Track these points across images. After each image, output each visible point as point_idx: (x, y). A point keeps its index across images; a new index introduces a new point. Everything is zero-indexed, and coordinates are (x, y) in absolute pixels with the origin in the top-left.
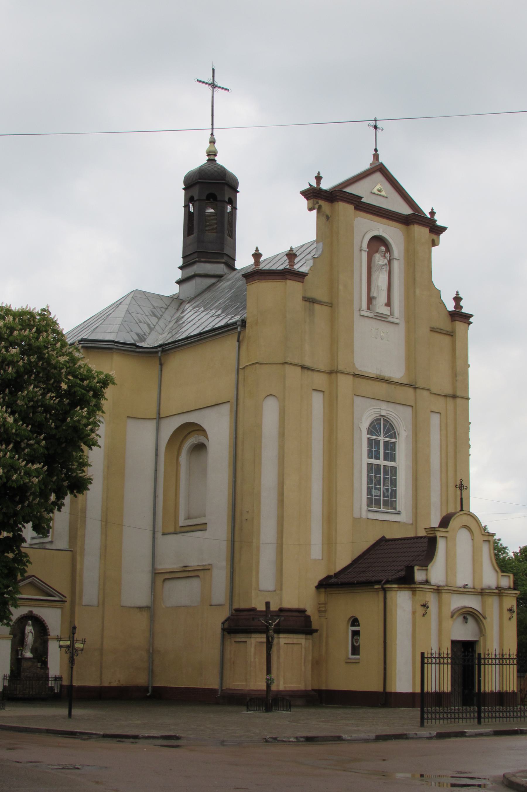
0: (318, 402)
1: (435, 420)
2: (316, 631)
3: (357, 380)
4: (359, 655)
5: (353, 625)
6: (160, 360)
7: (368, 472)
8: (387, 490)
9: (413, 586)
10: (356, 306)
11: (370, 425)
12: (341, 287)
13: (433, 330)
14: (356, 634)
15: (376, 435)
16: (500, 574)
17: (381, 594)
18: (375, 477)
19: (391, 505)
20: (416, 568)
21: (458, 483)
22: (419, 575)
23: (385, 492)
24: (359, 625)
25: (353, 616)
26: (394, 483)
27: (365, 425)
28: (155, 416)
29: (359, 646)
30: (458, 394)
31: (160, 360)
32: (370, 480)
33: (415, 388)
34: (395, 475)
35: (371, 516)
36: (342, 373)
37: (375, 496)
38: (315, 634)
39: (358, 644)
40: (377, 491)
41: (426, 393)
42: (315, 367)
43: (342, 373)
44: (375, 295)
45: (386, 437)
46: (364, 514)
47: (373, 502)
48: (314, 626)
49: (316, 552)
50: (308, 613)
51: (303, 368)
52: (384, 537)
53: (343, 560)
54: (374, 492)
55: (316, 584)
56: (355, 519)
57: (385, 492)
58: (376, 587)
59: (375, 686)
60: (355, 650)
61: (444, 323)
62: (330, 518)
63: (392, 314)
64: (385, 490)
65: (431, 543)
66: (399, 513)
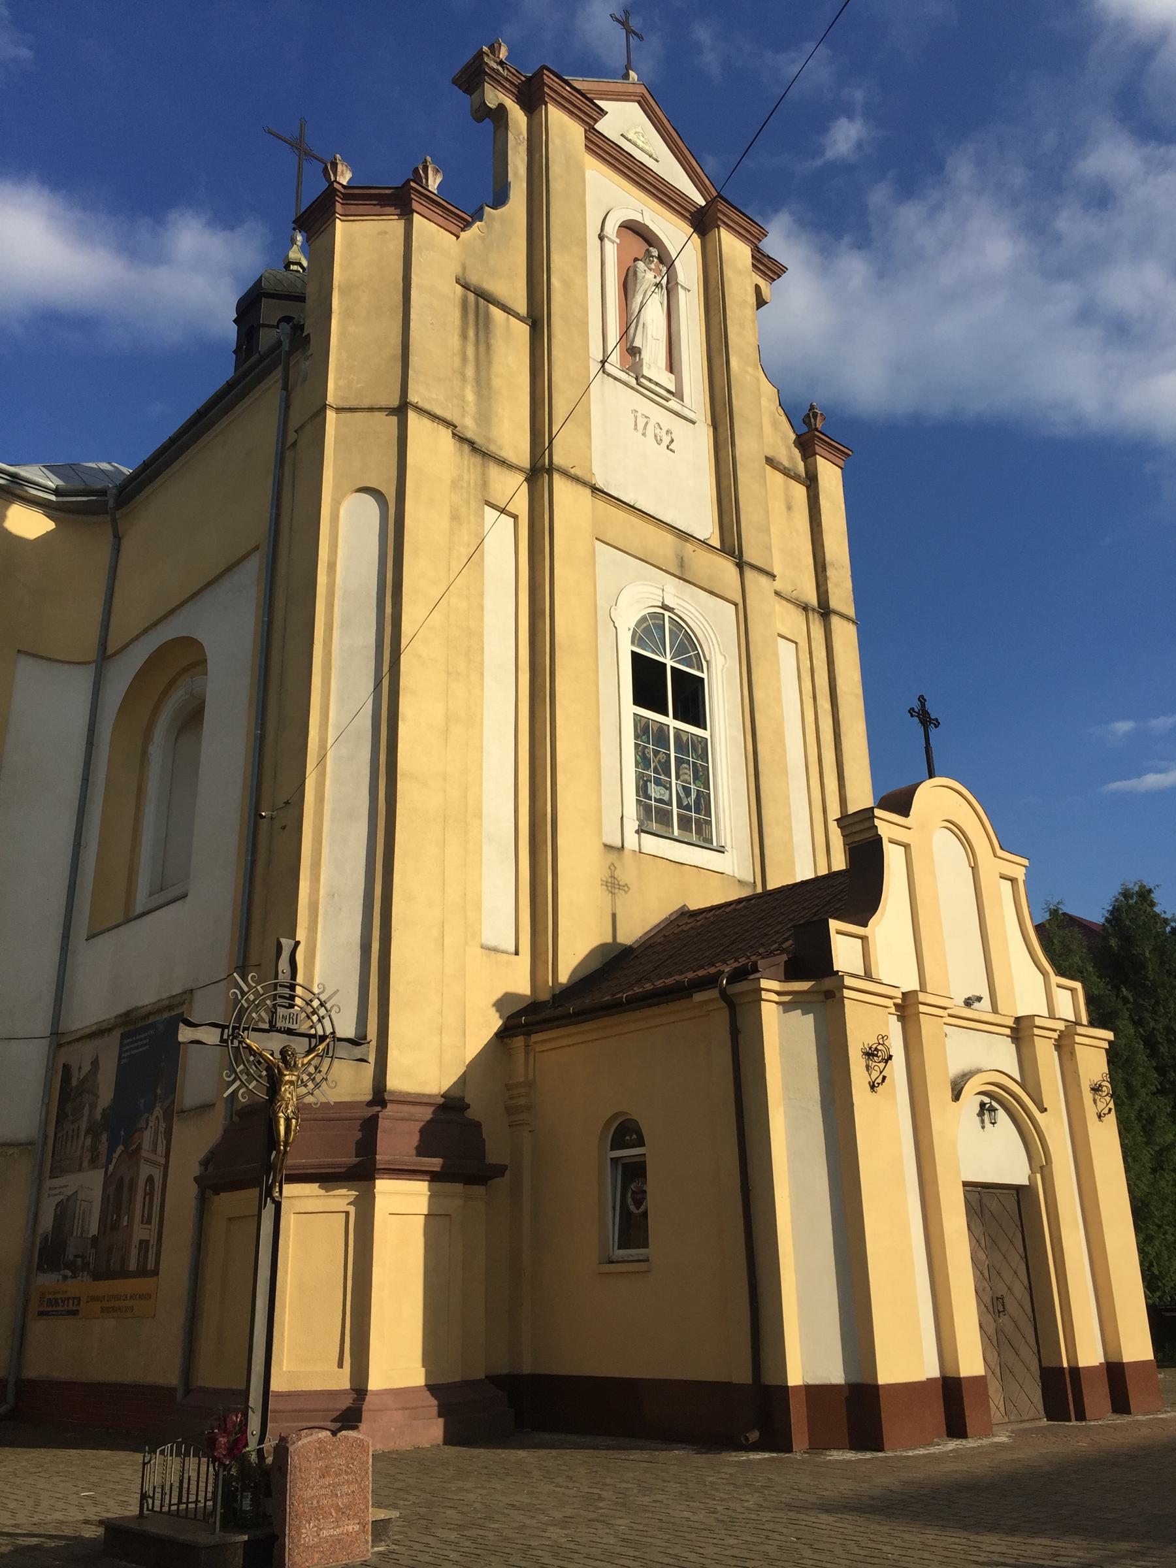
0: (502, 542)
1: (786, 652)
2: (500, 1170)
3: (602, 505)
4: (646, 1246)
5: (617, 1144)
6: (114, 521)
7: (637, 737)
8: (687, 791)
9: (827, 983)
11: (638, 624)
12: (555, 282)
13: (770, 461)
14: (634, 1172)
15: (653, 652)
16: (1055, 979)
18: (656, 753)
19: (699, 832)
20: (834, 925)
21: (916, 705)
22: (845, 952)
23: (683, 795)
24: (641, 1143)
25: (616, 1115)
26: (702, 775)
28: (92, 654)
29: (645, 1214)
31: (114, 521)
32: (642, 760)
33: (741, 565)
34: (704, 756)
35: (651, 844)
36: (565, 473)
37: (656, 800)
38: (500, 1184)
39: (641, 1210)
40: (662, 790)
41: (763, 580)
42: (493, 448)
43: (565, 473)
45: (678, 662)
47: (654, 818)
48: (496, 1151)
50: (473, 1113)
51: (461, 439)
54: (654, 791)
56: (608, 847)
57: (683, 795)
58: (699, 997)
59: (719, 1362)
60: (633, 1229)
61: (792, 457)
63: (678, 394)
64: (680, 789)
65: (866, 856)
66: (721, 850)
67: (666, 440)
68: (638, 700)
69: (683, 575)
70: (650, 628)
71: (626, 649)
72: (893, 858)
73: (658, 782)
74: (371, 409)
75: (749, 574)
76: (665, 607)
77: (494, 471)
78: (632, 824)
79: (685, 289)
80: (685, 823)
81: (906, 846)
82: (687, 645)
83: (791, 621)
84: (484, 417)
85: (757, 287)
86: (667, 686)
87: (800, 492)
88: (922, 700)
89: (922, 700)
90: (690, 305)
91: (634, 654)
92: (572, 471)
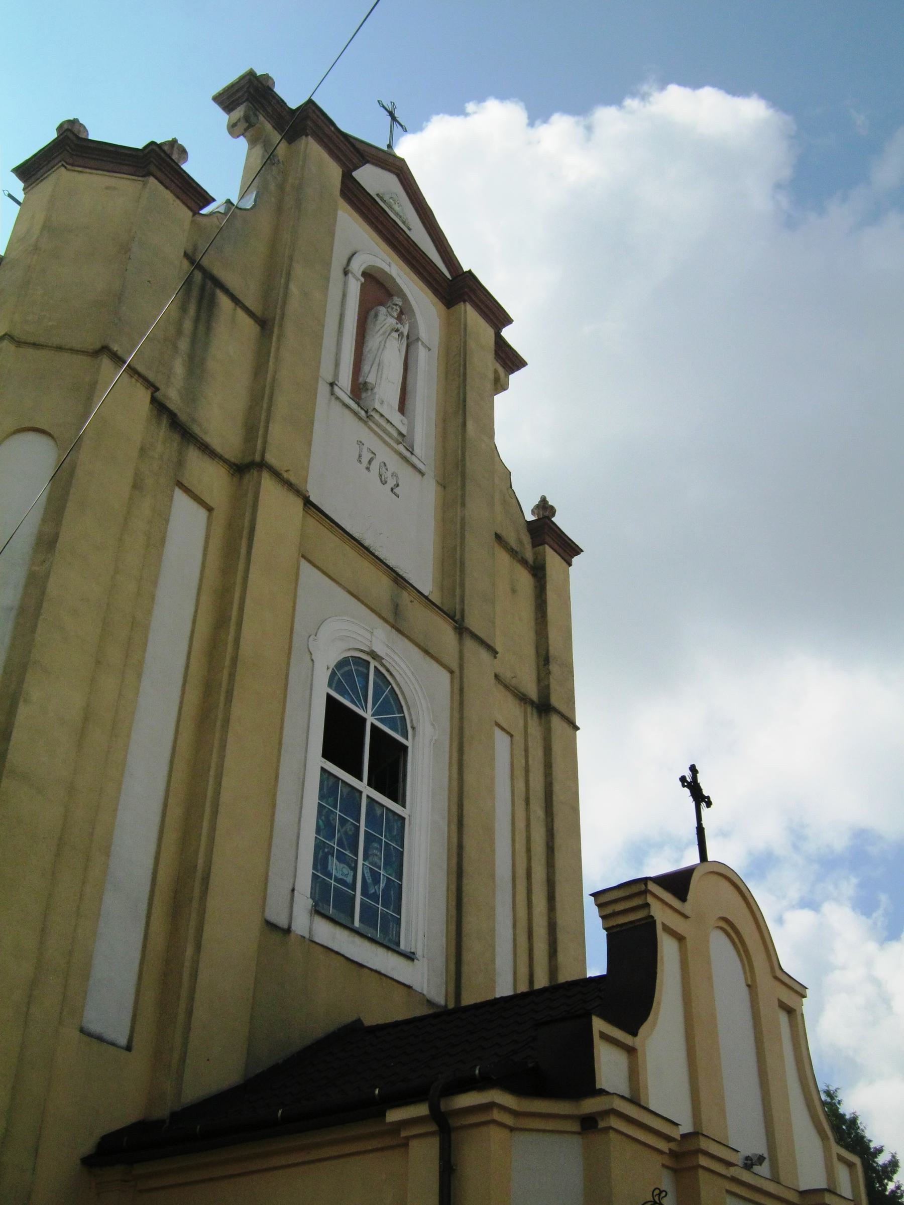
0: (188, 530)
1: (501, 742)
7: (322, 797)
8: (376, 877)
9: (590, 1106)
10: (326, 373)
12: (294, 288)
15: (353, 702)
17: (424, 1154)
18: (343, 821)
19: (385, 930)
20: (598, 1025)
22: (610, 1068)
23: (369, 881)
26: (395, 860)
27: (327, 657)
30: (555, 701)
32: (325, 826)
33: (461, 629)
34: (400, 839)
35: (326, 933)
36: (276, 474)
37: (337, 880)
40: (346, 870)
41: (484, 655)
42: (196, 429)
43: (276, 474)
44: (371, 379)
46: (302, 921)
47: (330, 902)
49: (112, 996)
51: (159, 407)
52: (359, 1021)
53: (215, 1064)
54: (336, 867)
55: (87, 1146)
56: (271, 926)
57: (369, 881)
58: (394, 1116)
62: (183, 892)
64: (367, 872)
66: (410, 957)
67: (391, 483)
68: (326, 754)
69: (396, 620)
70: (351, 672)
71: (321, 690)
72: (667, 949)
73: (341, 858)
74: (60, 348)
75: (470, 644)
76: (374, 655)
77: (193, 456)
78: (304, 901)
79: (425, 346)
80: (368, 915)
81: (680, 939)
82: (391, 702)
83: (510, 711)
84: (191, 394)
85: (496, 372)
86: (363, 746)
87: (525, 580)
88: (693, 769)
89: (693, 769)
90: (427, 363)
91: (329, 697)
92: (285, 475)
